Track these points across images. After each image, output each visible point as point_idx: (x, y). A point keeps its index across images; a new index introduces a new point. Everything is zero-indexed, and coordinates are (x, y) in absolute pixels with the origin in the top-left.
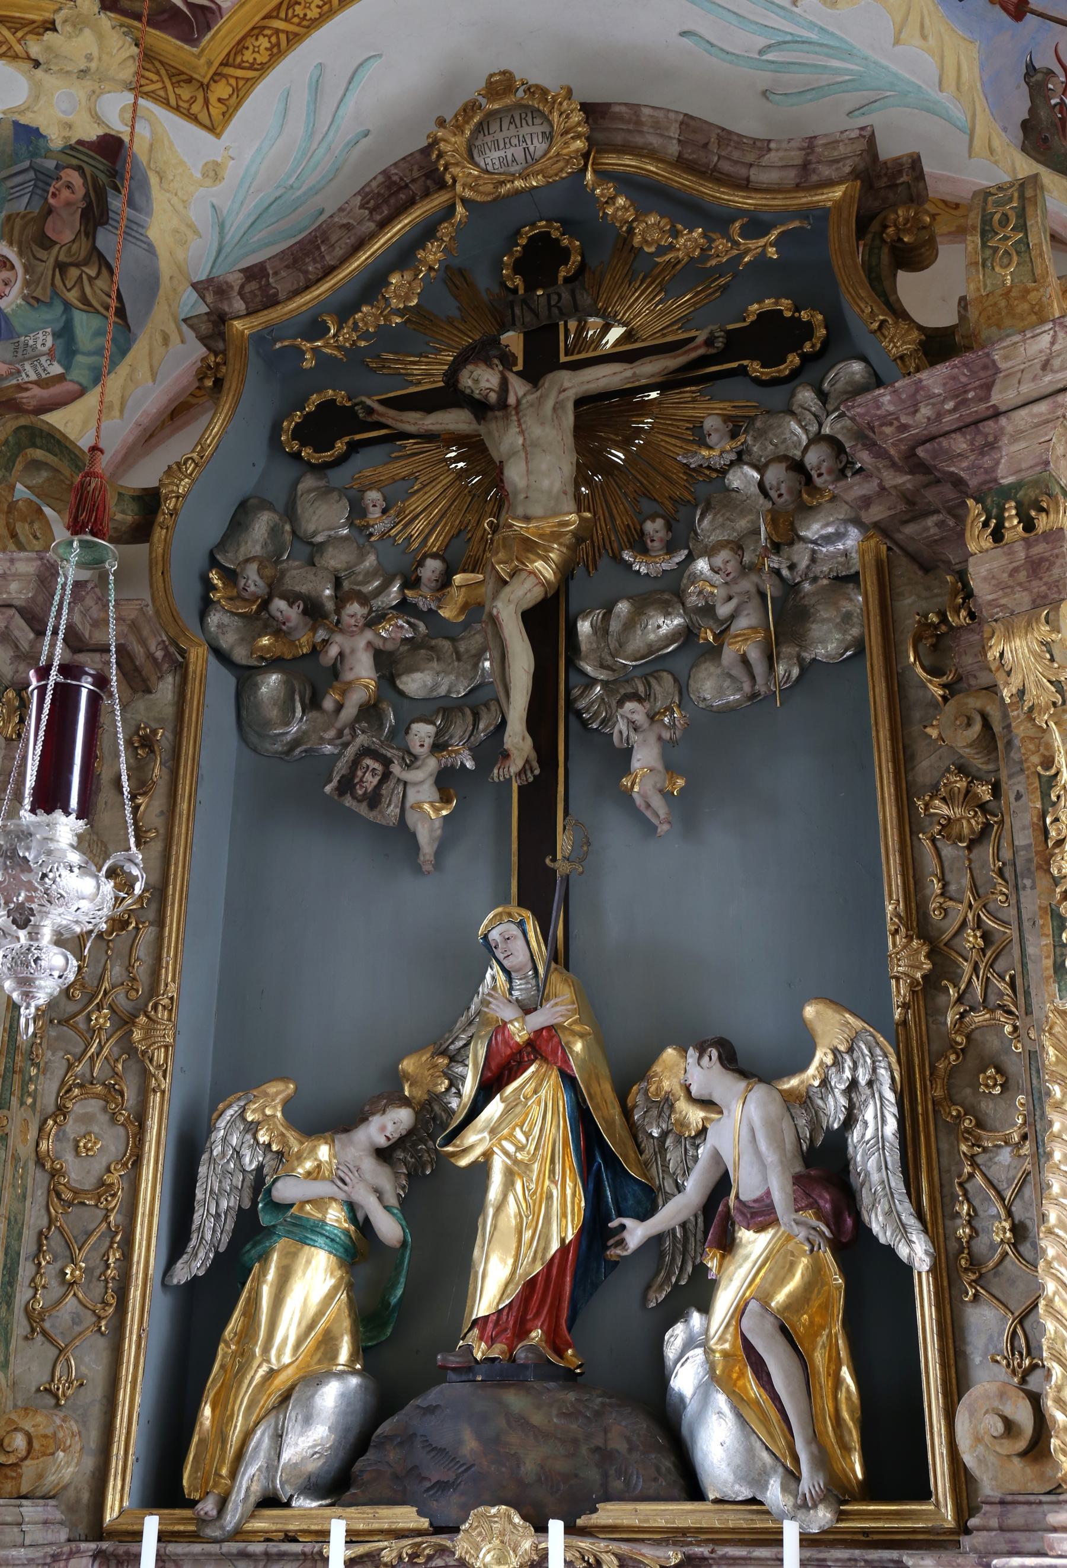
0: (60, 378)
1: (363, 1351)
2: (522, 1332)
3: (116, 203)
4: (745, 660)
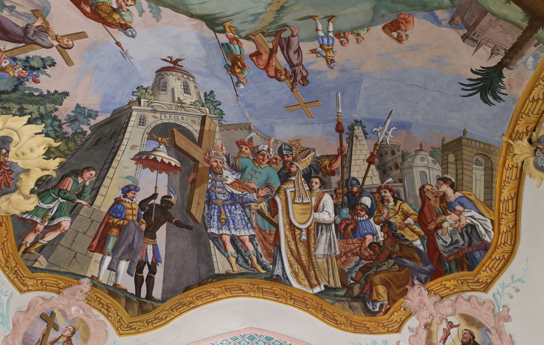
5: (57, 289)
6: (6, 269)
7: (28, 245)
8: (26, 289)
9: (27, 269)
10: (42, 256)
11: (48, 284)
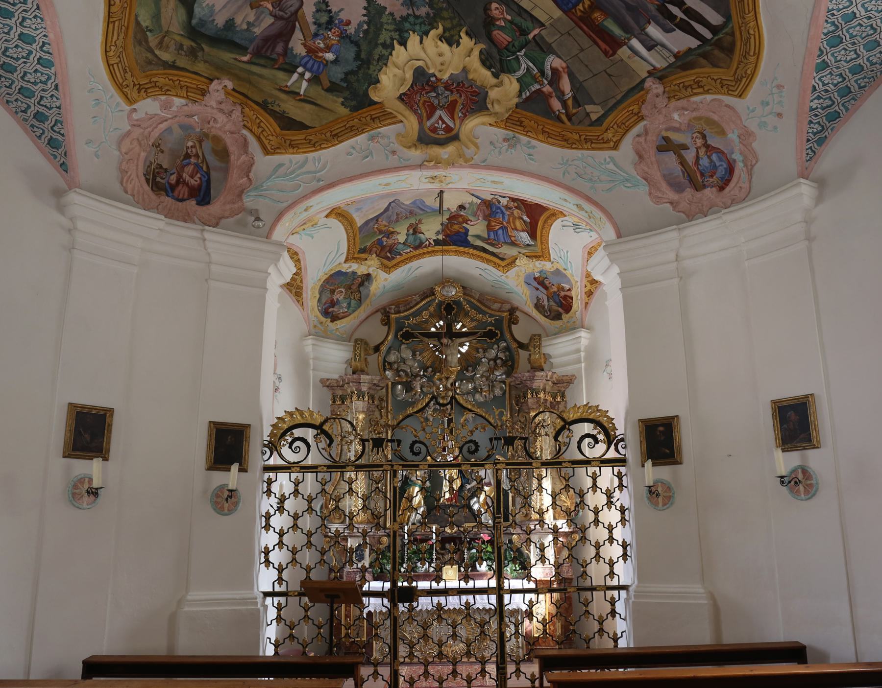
1: (425, 503)
3: (366, 283)
5: (636, 117)
6: (574, 146)
8: (612, 144)
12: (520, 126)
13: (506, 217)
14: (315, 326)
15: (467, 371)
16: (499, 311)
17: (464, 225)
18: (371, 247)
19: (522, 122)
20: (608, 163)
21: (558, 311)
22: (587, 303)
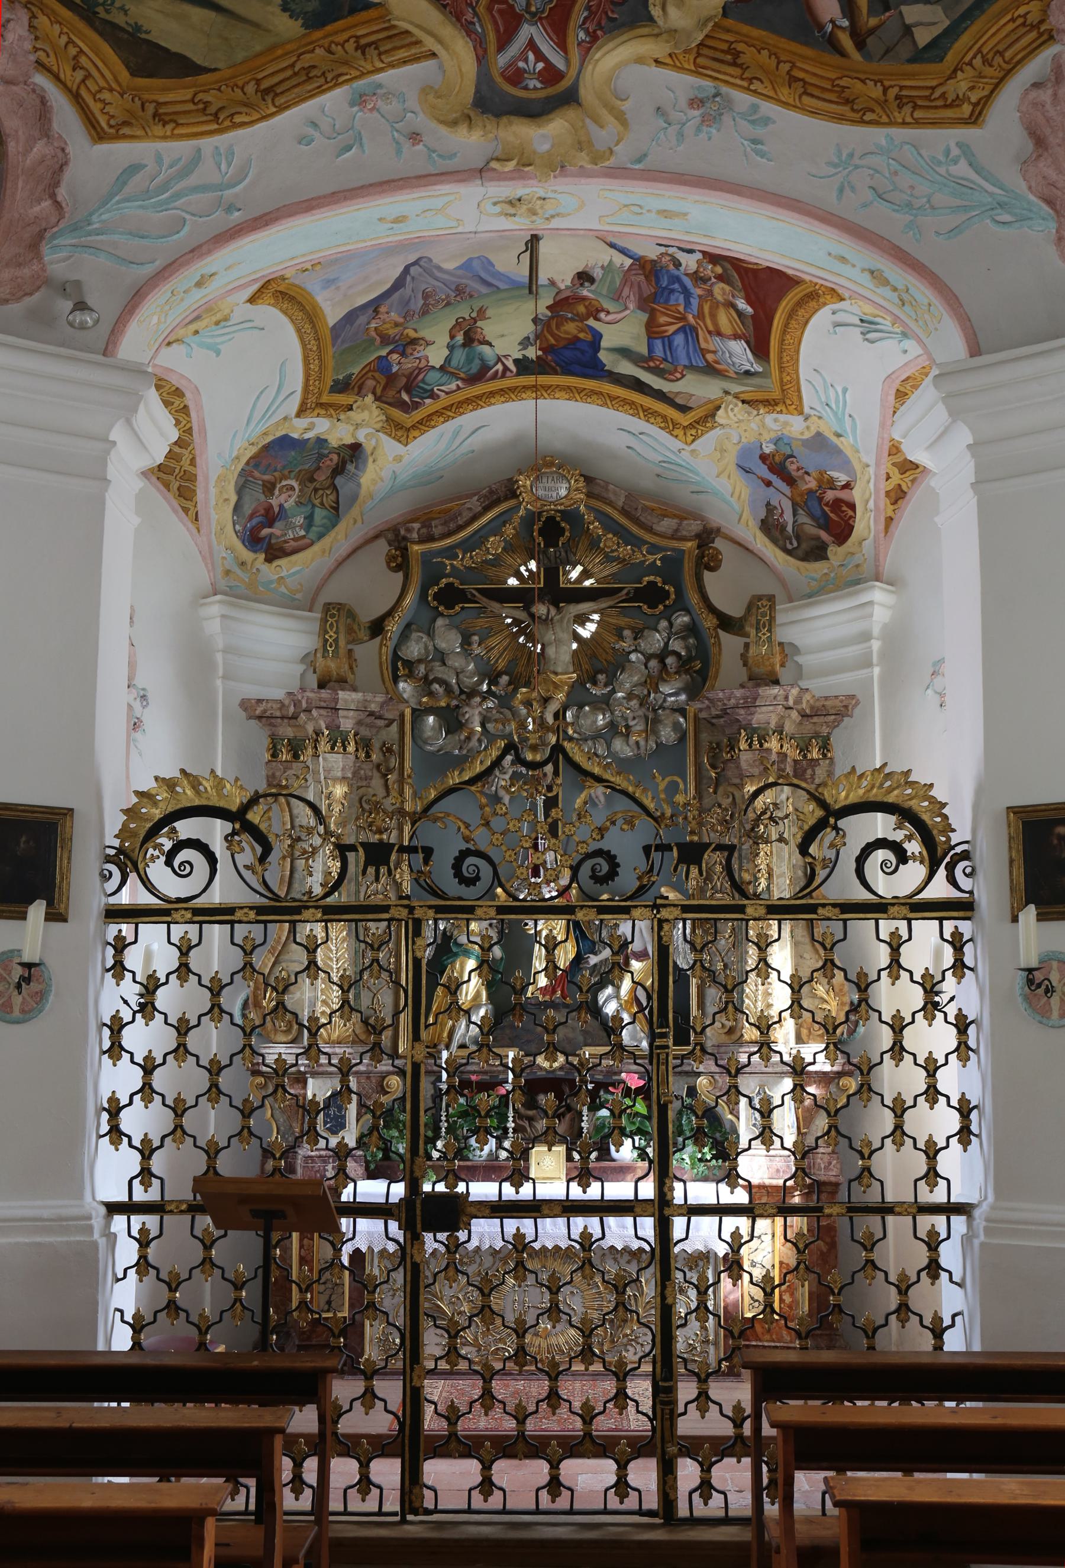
0: (304, 537)
2: (554, 992)
3: (350, 467)
4: (637, 743)
5: (1034, 34)
6: (869, 116)
7: (845, 23)
8: (966, 109)
9: (916, 67)
10: (904, 9)
11: (1001, 48)
12: (734, 64)
13: (695, 302)
14: (228, 572)
15: (595, 683)
16: (673, 537)
17: (591, 322)
18: (363, 376)
19: (737, 54)
20: (955, 162)
21: (818, 538)
22: (889, 520)
